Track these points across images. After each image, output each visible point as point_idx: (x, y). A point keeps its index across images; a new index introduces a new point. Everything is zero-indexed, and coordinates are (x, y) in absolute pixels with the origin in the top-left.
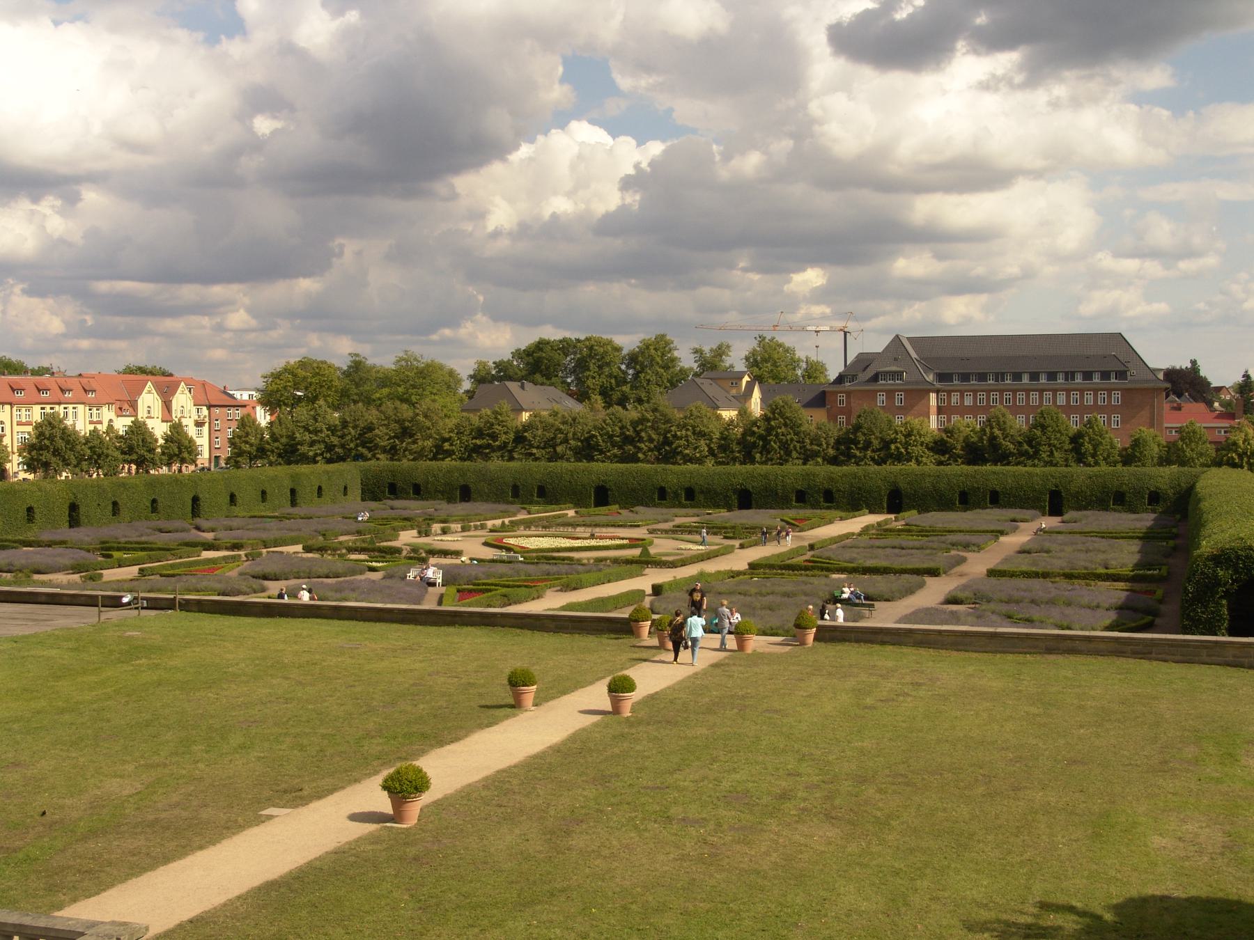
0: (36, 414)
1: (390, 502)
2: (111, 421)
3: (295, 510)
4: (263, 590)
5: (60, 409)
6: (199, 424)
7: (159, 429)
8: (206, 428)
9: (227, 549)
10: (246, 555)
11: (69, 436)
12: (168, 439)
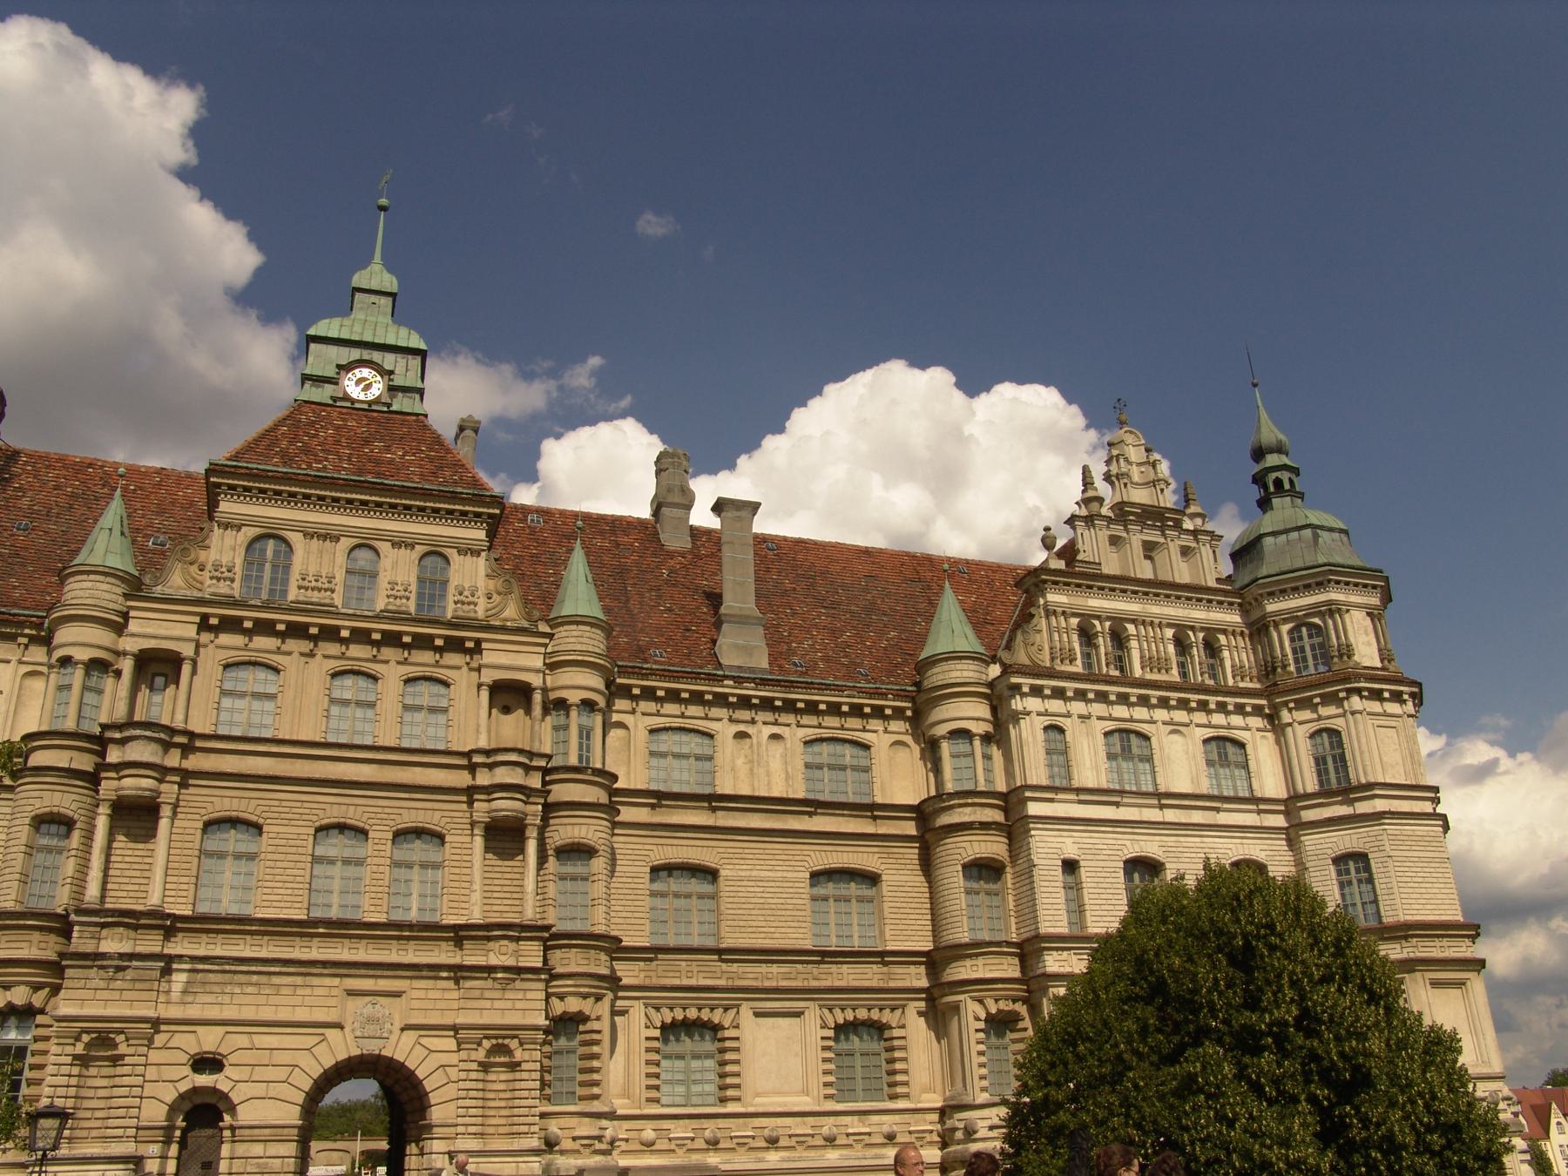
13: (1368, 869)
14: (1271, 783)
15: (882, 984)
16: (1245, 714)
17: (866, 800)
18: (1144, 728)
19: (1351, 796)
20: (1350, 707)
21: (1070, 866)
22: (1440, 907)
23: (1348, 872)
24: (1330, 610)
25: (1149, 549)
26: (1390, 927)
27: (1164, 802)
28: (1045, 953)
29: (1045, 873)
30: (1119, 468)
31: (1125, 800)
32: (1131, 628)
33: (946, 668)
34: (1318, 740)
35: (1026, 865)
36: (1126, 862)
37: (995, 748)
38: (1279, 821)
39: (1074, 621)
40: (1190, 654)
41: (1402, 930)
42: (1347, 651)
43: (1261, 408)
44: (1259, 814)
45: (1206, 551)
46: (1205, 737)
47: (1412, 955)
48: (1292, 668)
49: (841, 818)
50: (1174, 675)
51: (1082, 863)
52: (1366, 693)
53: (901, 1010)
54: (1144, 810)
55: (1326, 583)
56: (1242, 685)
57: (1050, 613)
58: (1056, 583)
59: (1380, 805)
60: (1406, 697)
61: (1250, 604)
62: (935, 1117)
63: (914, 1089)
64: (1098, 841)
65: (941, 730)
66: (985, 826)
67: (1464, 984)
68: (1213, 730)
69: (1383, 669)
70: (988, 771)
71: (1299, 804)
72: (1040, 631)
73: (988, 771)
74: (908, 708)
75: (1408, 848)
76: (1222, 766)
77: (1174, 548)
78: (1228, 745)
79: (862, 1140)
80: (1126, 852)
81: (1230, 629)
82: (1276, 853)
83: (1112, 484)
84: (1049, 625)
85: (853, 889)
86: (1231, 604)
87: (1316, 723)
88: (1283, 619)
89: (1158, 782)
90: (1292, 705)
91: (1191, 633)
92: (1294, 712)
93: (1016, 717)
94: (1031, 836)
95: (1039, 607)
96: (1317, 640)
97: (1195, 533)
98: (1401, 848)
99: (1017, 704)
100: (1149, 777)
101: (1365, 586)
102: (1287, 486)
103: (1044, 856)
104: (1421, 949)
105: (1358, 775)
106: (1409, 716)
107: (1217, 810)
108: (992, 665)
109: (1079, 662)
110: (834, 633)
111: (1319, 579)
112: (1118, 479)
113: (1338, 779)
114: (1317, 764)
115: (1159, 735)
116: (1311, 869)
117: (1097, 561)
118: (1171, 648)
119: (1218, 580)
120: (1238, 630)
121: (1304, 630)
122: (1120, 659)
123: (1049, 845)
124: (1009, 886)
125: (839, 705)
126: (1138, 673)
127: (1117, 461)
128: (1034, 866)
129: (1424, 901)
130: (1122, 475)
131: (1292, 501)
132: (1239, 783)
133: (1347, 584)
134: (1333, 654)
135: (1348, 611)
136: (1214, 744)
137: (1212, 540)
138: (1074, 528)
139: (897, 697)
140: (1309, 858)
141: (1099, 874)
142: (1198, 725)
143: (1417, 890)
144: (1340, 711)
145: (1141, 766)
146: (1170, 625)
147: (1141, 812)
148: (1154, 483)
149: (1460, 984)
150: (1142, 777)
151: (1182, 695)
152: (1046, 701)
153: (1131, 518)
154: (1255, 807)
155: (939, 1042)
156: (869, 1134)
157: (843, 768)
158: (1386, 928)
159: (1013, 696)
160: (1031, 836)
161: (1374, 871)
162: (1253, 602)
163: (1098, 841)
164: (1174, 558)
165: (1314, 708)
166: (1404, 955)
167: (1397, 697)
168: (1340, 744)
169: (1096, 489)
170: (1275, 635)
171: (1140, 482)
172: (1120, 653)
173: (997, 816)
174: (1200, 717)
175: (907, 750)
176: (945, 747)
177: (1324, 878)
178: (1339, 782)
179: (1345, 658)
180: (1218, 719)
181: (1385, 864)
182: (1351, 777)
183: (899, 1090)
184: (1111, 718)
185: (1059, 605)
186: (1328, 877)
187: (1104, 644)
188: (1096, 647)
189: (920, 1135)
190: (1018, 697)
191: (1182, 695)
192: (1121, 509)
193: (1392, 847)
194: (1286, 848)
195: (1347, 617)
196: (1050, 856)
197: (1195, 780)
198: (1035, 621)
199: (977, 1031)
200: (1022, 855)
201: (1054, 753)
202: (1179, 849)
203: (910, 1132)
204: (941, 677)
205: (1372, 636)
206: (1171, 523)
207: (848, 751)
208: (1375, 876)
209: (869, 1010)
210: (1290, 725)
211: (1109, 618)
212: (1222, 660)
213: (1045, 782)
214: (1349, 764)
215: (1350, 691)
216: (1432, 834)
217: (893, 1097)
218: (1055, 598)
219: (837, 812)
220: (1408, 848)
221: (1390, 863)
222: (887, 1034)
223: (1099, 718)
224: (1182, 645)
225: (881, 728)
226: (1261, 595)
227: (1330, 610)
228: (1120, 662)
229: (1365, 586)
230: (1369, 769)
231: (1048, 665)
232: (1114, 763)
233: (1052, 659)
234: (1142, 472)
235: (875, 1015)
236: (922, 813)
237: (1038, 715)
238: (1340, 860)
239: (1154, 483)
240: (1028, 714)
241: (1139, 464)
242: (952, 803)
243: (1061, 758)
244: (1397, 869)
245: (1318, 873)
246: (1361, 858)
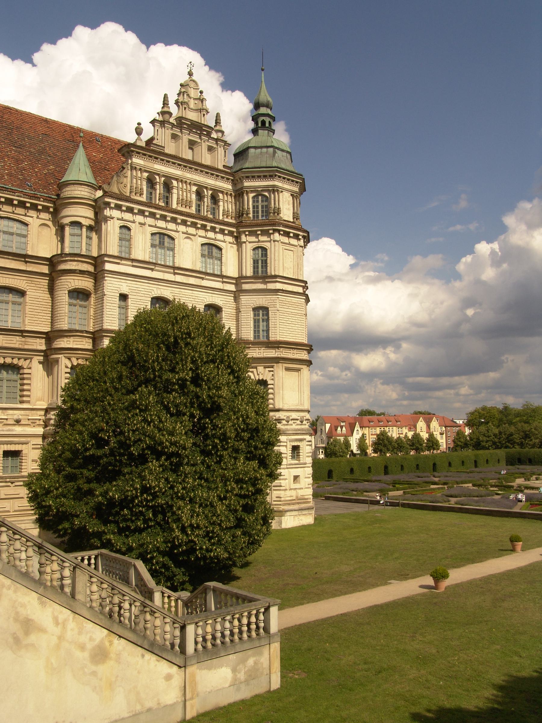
0: (378, 431)
1: (518, 466)
2: (406, 433)
3: (477, 469)
4: (449, 501)
5: (387, 429)
6: (441, 434)
7: (425, 435)
8: (444, 435)
9: (442, 485)
10: (447, 487)
11: (389, 440)
12: (428, 440)
13: (268, 315)
14: (231, 270)
15: (20, 347)
16: (224, 234)
17: (23, 252)
18: (172, 234)
19: (266, 280)
20: (274, 238)
21: (124, 297)
22: (296, 336)
23: (259, 315)
24: (273, 190)
25: (192, 144)
26: (272, 342)
27: (176, 271)
28: (104, 338)
29: (110, 299)
30: (184, 99)
31: (157, 268)
32: (175, 183)
33: (73, 188)
34: (257, 252)
35: (101, 294)
36: (152, 298)
37: (94, 234)
38: (232, 288)
39: (146, 175)
40: (203, 201)
41: (277, 344)
42: (278, 211)
43: (263, 82)
44: (223, 283)
45: (221, 150)
46: (203, 243)
47: (279, 356)
48: (251, 215)
49: (7, 260)
50: (193, 210)
51: (130, 296)
52: (282, 233)
53: (29, 360)
54: (166, 274)
55: (274, 176)
56: (226, 220)
57: (133, 168)
58: (139, 153)
59: (279, 286)
60: (300, 237)
61: (237, 181)
62: (43, 413)
63: (32, 399)
64: (140, 286)
65: (66, 221)
66: (82, 272)
67: (300, 370)
68: (207, 240)
69: (293, 222)
70: (89, 245)
71: (242, 281)
72: (126, 177)
73: (89, 245)
74: (51, 207)
75: (287, 307)
76: (209, 258)
77: (205, 146)
78: (214, 248)
79: (2, 422)
80: (153, 293)
81: (225, 191)
82: (228, 303)
83: (178, 106)
84: (132, 174)
85: (11, 297)
86: (228, 179)
87: (257, 244)
88: (251, 191)
89: (175, 262)
90: (247, 233)
91: (205, 190)
92: (248, 236)
93: (106, 219)
94: (105, 280)
95: (128, 164)
96: (265, 204)
97: (217, 140)
98: (284, 307)
99: (107, 212)
100: (171, 258)
101: (293, 181)
102: (267, 125)
103: (111, 291)
105: (271, 271)
106: (300, 246)
107: (203, 279)
108: (98, 191)
109: (145, 196)
110: (18, 161)
111: (271, 174)
112: (182, 105)
113: (262, 271)
114: (254, 263)
115: (179, 238)
116: (242, 312)
117: (163, 145)
118: (194, 196)
119: (224, 166)
120: (229, 193)
121: (260, 197)
122: (167, 198)
123: (114, 285)
124: (92, 304)
125: (12, 200)
126: (174, 206)
127: (183, 95)
128: (105, 295)
129: (289, 332)
130: (184, 103)
131: (268, 133)
132: (216, 267)
133: (284, 178)
134: (271, 211)
135: (282, 192)
136: (206, 247)
137: (225, 145)
138: (154, 126)
139: (45, 200)
140: (242, 307)
141: (138, 303)
142: (200, 236)
143: (288, 327)
144: (269, 239)
145: (168, 252)
146: (195, 185)
147: (164, 275)
148: (200, 110)
149: (298, 370)
150: (168, 258)
151: (194, 220)
152: (123, 213)
153: (185, 126)
154: (221, 280)
155: (48, 377)
156: (7, 419)
157: (12, 234)
158: (270, 342)
159: (106, 208)
160: (105, 280)
161: (270, 316)
162: (239, 180)
163: (140, 286)
164: (203, 151)
165: (257, 236)
166: (276, 355)
167: (296, 237)
168: (266, 255)
169: (169, 108)
170: (246, 198)
171: (193, 108)
172: (168, 195)
173: (91, 269)
174: (202, 233)
175: (49, 229)
176: (67, 229)
177: (247, 317)
178: (262, 273)
179: (276, 214)
180: (211, 235)
181: (275, 314)
182: (268, 271)
183: (25, 399)
184: (156, 227)
185: (139, 165)
186: (249, 317)
187: (159, 189)
188: (155, 190)
189: (34, 421)
190: (108, 209)
191: (194, 220)
192: (180, 121)
193: (280, 306)
194: (233, 301)
195: (281, 194)
196: (114, 291)
197: (194, 263)
198: (125, 171)
199: (66, 373)
200: (100, 289)
201: (124, 240)
202: (180, 295)
203: (29, 419)
204: (69, 193)
205: (292, 205)
206: (205, 133)
207: (16, 225)
208: (270, 318)
209: (13, 359)
210: (245, 242)
211: (164, 176)
212: (219, 206)
213: (116, 254)
214: (268, 265)
215: (275, 230)
216: (300, 302)
217: (22, 402)
218: (137, 160)
219: (5, 257)
220: (287, 307)
221: (278, 313)
222: (21, 371)
223: (150, 226)
224: (200, 195)
225: (35, 216)
226: (243, 177)
227: (273, 190)
228: (167, 200)
229: (293, 181)
230: (277, 268)
231: (128, 195)
232: (154, 250)
233: (131, 192)
234: (196, 104)
235: (15, 361)
236: (52, 262)
237: (118, 219)
238: (256, 309)
239: (200, 110)
240: (113, 218)
241: (195, 99)
242: (67, 259)
243: (127, 243)
244: (280, 316)
245: (245, 314)
246: (265, 309)
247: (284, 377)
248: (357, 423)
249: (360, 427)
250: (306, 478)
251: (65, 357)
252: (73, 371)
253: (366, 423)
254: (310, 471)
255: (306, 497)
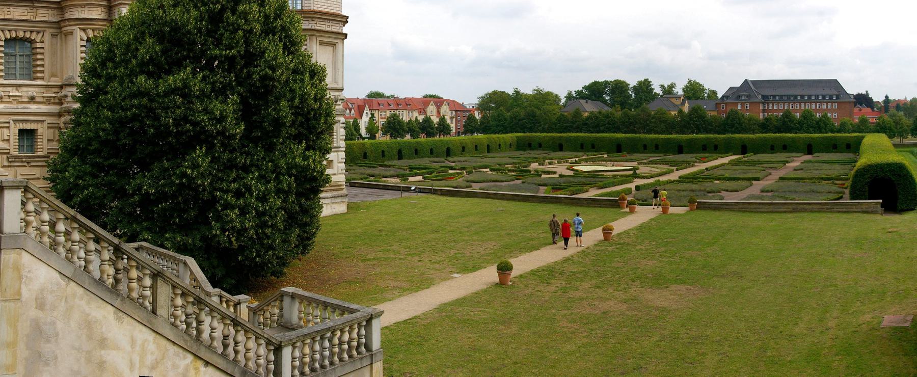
0: (388, 114)
1: (528, 151)
2: (416, 117)
3: (489, 155)
4: (471, 187)
5: (397, 112)
6: (452, 118)
8: (454, 119)
9: (459, 170)
10: (466, 172)
11: (400, 122)
12: (439, 124)
15: (32, 19)
53: (41, 34)
104: (318, 25)
149: (333, 45)
199: (82, 46)
222: (34, 46)
247: (318, 51)
248: (367, 106)
249: (370, 110)
250: (339, 163)
251: (79, 28)
252: (88, 43)
253: (375, 106)
254: (342, 155)
255: (340, 183)
